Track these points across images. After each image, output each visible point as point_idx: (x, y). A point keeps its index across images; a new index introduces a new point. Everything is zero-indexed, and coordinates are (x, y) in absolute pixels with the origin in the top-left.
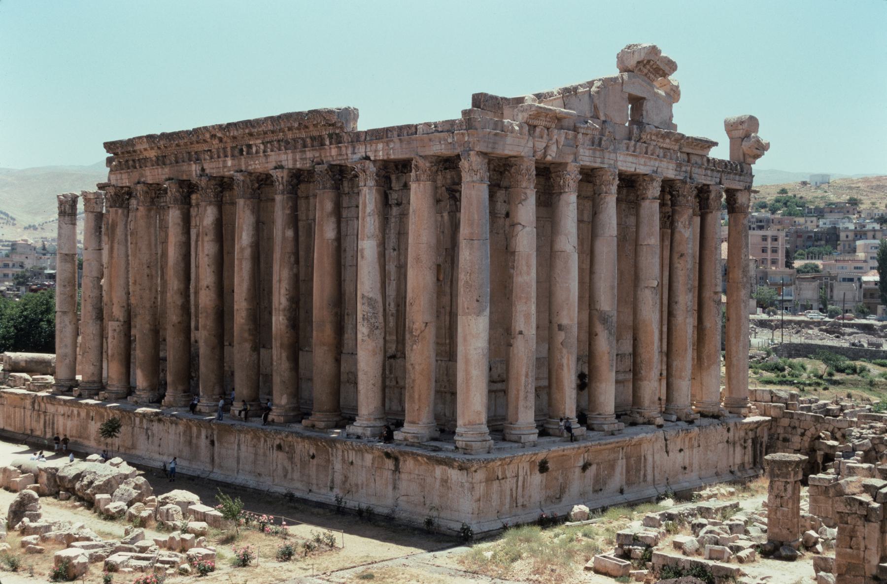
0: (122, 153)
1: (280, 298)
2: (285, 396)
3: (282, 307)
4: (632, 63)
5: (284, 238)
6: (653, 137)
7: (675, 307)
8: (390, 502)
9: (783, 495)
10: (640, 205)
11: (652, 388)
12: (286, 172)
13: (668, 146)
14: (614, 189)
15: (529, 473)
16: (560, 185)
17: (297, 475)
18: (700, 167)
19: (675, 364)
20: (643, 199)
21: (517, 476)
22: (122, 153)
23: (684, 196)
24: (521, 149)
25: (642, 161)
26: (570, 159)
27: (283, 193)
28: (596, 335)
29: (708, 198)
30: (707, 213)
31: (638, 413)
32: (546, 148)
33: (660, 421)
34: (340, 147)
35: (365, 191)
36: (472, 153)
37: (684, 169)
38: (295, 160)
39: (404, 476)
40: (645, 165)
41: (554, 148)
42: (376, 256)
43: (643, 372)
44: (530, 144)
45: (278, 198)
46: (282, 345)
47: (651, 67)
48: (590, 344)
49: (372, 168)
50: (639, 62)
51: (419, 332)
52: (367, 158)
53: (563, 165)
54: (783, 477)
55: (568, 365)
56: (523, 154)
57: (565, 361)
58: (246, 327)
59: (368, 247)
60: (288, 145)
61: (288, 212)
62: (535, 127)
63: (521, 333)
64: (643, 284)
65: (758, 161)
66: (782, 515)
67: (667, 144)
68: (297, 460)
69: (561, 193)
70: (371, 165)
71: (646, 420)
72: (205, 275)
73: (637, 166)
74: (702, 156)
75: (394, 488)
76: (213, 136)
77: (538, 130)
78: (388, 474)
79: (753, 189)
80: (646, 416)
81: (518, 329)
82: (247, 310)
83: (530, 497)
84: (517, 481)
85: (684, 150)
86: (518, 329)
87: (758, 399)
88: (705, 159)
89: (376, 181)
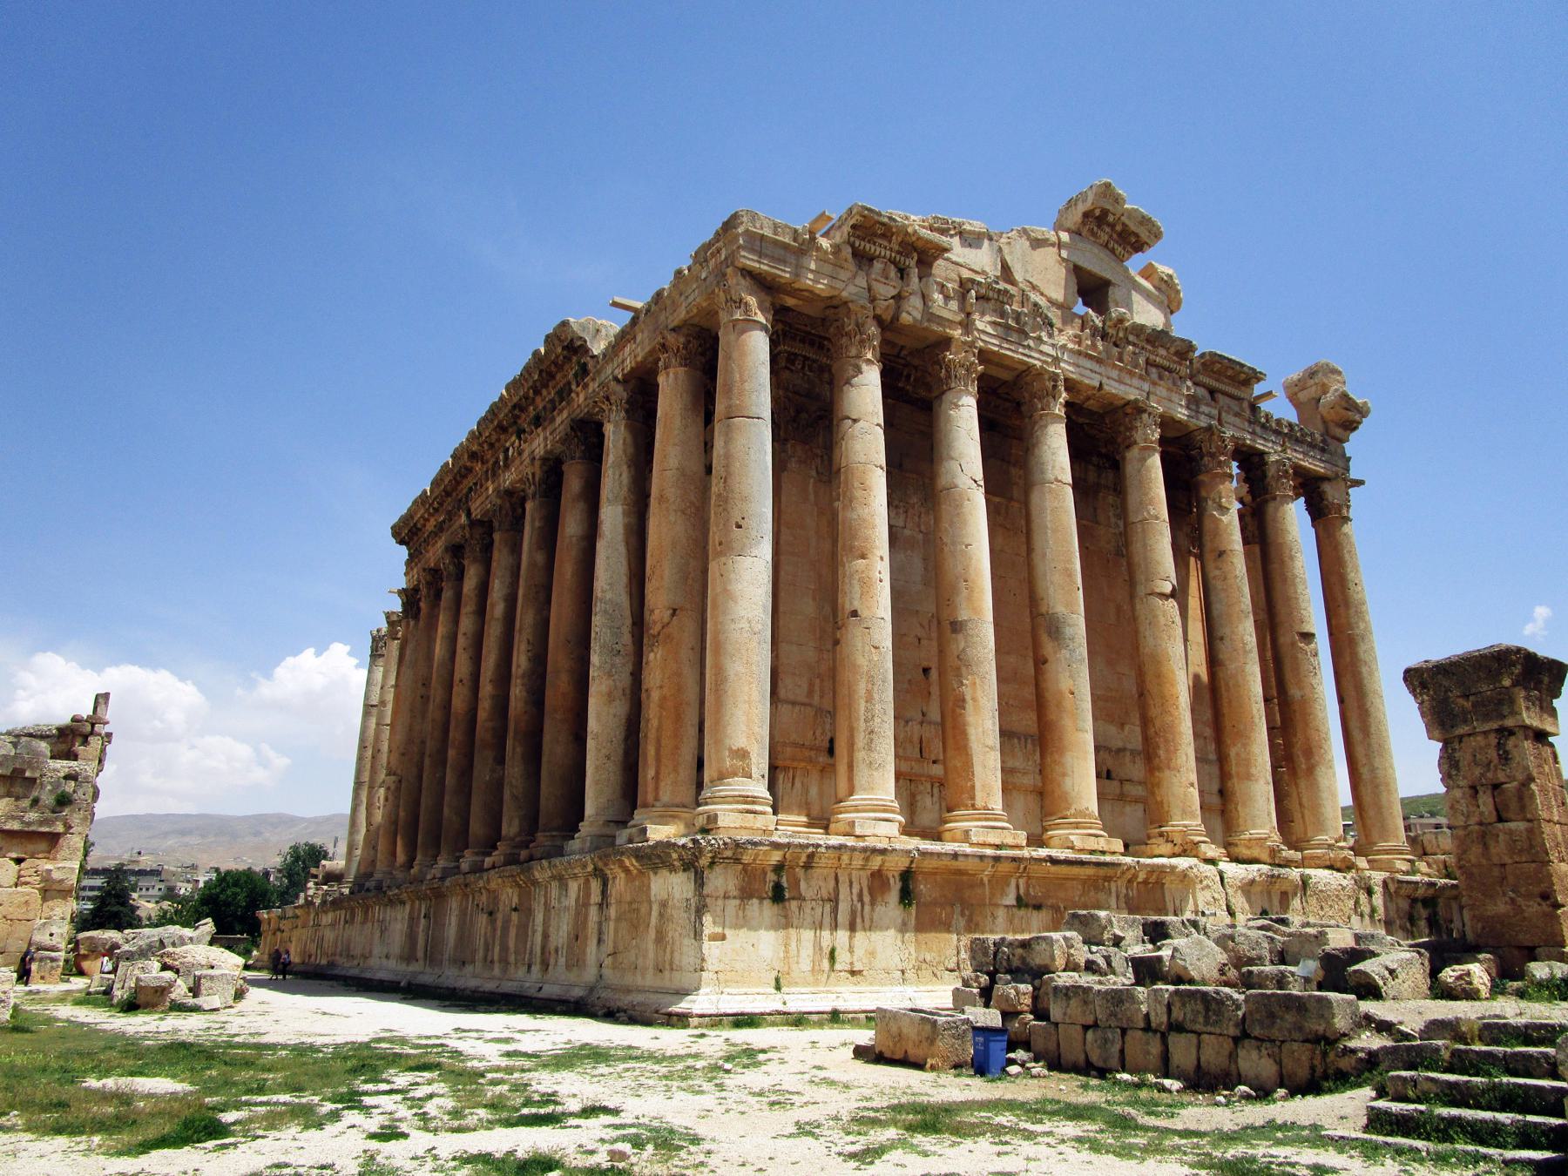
0: (407, 532)
1: (521, 660)
2: (516, 822)
3: (521, 671)
4: (1076, 216)
5: (532, 564)
6: (1131, 338)
7: (1221, 646)
8: (590, 974)
9: (1501, 777)
10: (1124, 458)
11: (1184, 781)
12: (537, 463)
13: (1166, 363)
14: (1059, 410)
15: (867, 899)
16: (940, 379)
17: (497, 949)
18: (1237, 415)
19: (1233, 752)
20: (1128, 447)
21: (834, 900)
22: (407, 532)
23: (1213, 455)
24: (840, 285)
25: (1114, 373)
26: (957, 333)
27: (534, 497)
28: (1045, 662)
29: (1264, 476)
30: (1266, 501)
31: (1161, 835)
32: (898, 298)
33: (1211, 850)
34: (586, 386)
35: (609, 429)
36: (729, 270)
37: (1204, 408)
38: (546, 439)
39: (613, 912)
40: (1120, 381)
41: (915, 302)
42: (621, 529)
43: (1161, 753)
44: (861, 281)
45: (529, 506)
46: (516, 732)
47: (1112, 226)
48: (1037, 685)
49: (620, 392)
50: (1086, 215)
51: (657, 628)
52: (616, 379)
53: (946, 342)
54: (1487, 717)
55: (974, 699)
56: (844, 294)
57: (968, 692)
58: (490, 724)
59: (612, 517)
60: (538, 421)
61: (537, 524)
62: (871, 259)
63: (855, 614)
64: (1141, 590)
65: (1353, 436)
66: (1512, 850)
67: (1161, 355)
68: (499, 924)
69: (943, 393)
70: (619, 389)
71: (1177, 849)
72: (462, 667)
73: (1105, 380)
74: (1239, 399)
75: (600, 941)
76: (473, 456)
77: (878, 265)
78: (593, 912)
79: (1353, 475)
80: (1178, 840)
81: (848, 608)
82: (493, 697)
83: (872, 954)
84: (835, 911)
85: (1201, 378)
86: (848, 608)
87: (1429, 849)
88: (1245, 404)
89: (627, 411)
